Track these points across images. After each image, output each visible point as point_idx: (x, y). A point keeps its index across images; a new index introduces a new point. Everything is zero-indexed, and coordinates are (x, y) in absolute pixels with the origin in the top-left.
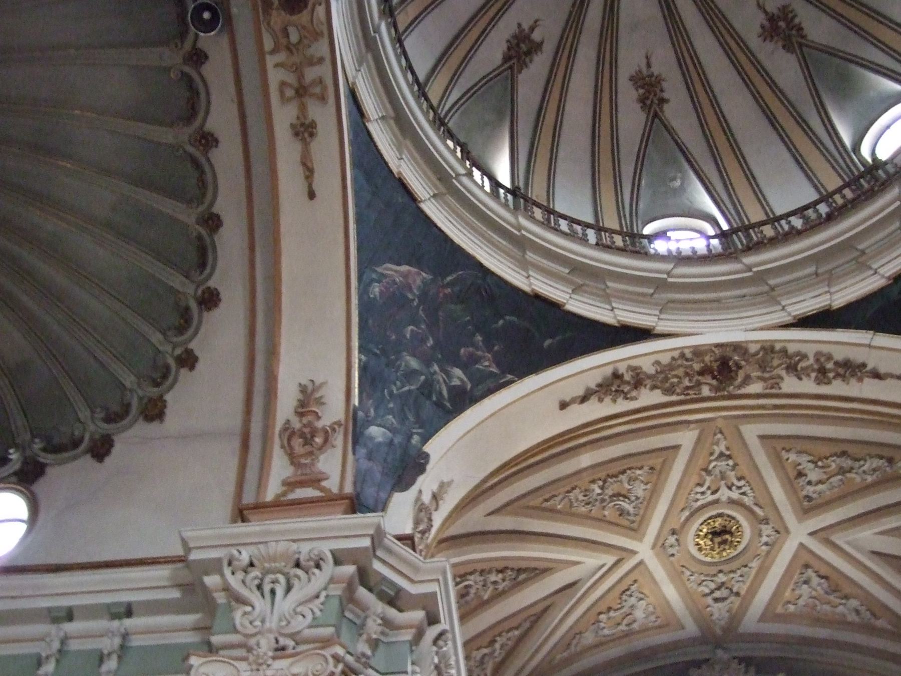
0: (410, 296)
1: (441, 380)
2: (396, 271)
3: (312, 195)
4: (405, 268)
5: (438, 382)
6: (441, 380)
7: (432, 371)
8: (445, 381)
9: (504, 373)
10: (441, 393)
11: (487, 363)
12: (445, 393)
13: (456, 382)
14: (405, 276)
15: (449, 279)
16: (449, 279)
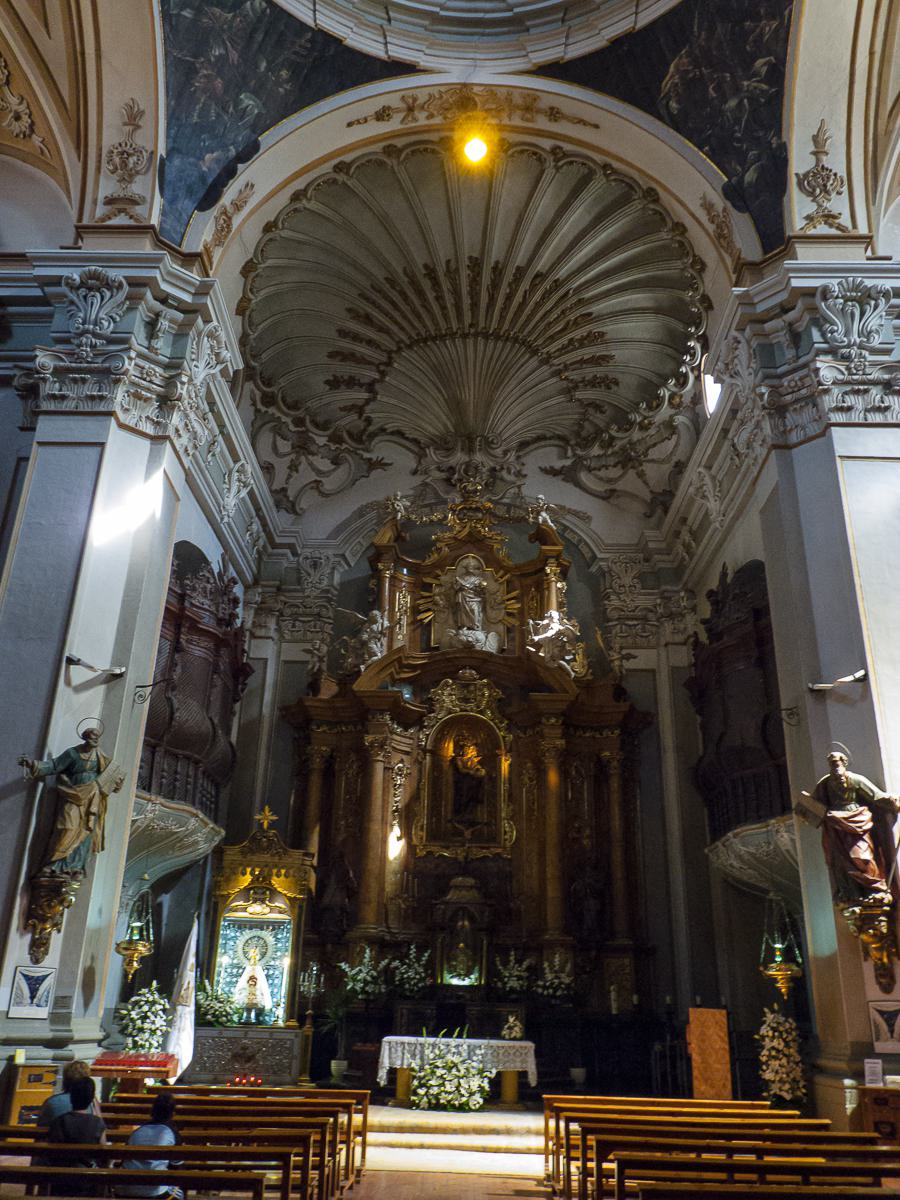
0: (691, 75)
1: (755, 84)
2: (671, 77)
3: (597, 126)
4: (672, 69)
5: (755, 88)
6: (755, 84)
7: (746, 89)
8: (758, 81)
9: (782, 16)
10: (762, 91)
11: (767, 29)
12: (765, 87)
13: (764, 69)
14: (677, 68)
15: (695, 29)
16: (695, 29)
